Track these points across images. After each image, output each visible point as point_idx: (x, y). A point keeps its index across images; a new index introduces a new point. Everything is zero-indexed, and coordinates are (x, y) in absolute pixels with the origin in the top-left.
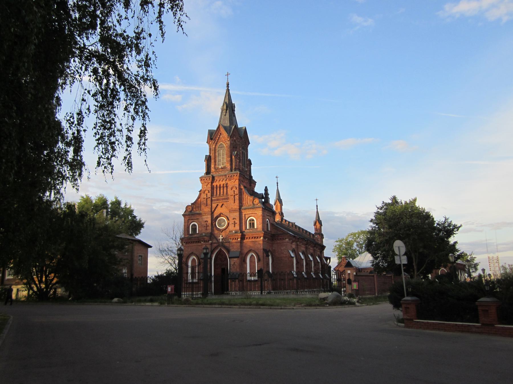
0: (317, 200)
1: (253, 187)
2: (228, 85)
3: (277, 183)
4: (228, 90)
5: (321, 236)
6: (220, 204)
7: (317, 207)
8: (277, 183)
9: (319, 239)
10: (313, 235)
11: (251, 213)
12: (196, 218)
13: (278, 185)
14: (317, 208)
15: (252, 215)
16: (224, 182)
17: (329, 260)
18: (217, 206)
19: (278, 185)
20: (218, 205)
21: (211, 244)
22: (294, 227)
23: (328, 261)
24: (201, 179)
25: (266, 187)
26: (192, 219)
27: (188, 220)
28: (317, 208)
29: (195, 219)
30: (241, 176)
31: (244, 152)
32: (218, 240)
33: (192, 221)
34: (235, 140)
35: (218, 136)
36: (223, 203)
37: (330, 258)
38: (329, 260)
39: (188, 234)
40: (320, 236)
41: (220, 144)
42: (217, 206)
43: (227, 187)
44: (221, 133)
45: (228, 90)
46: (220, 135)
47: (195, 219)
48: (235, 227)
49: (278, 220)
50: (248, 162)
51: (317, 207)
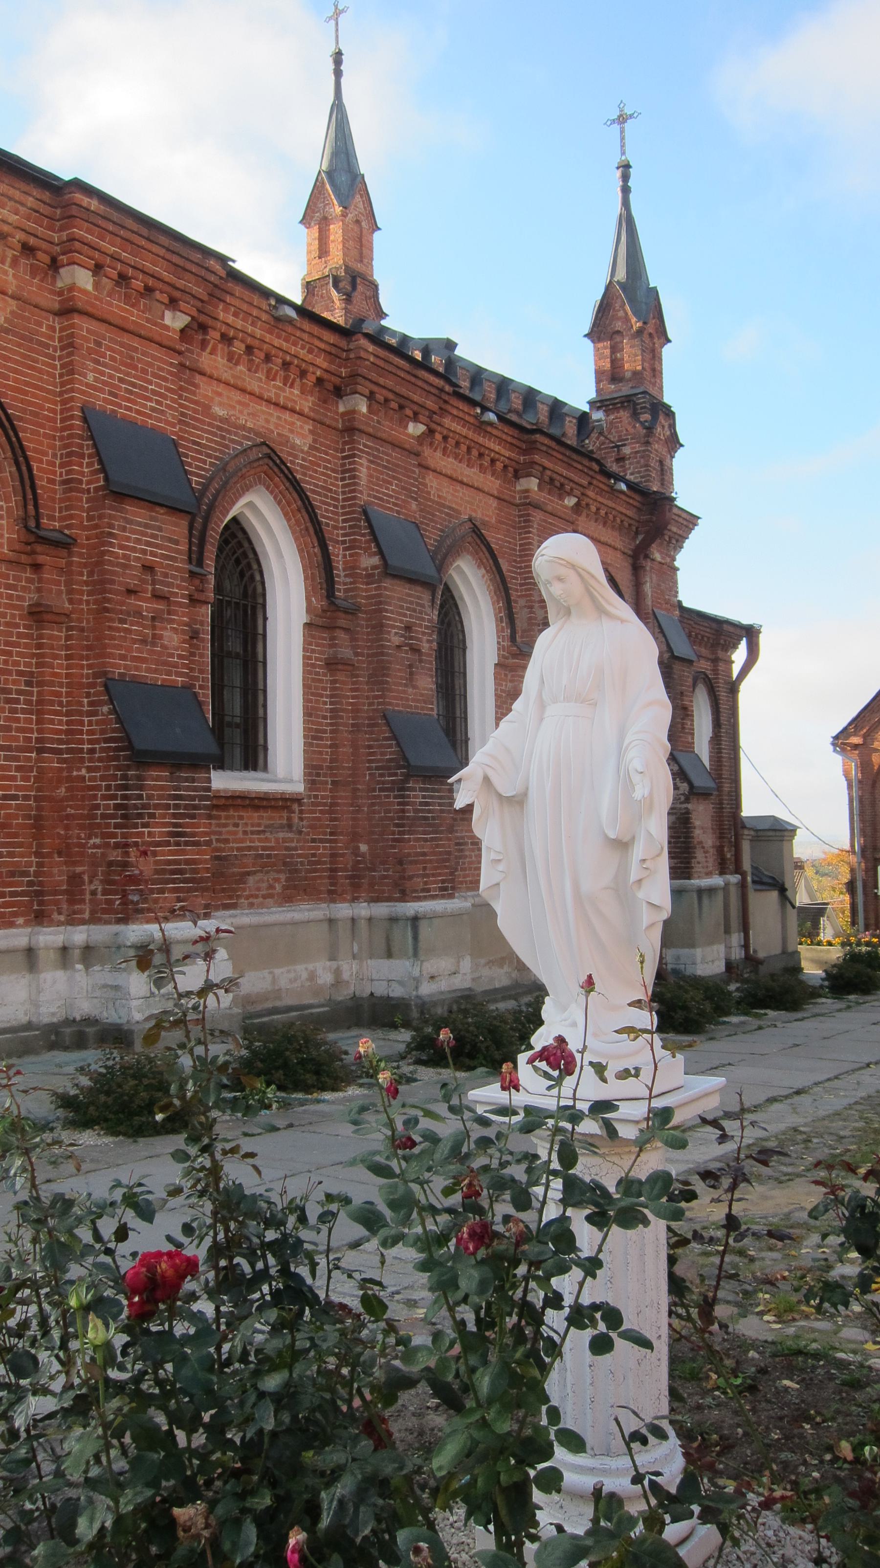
0: (622, 119)
3: (338, 58)
5: (646, 417)
7: (625, 177)
8: (338, 58)
9: (627, 450)
10: (583, 419)
13: (338, 73)
14: (626, 190)
17: (743, 645)
19: (338, 73)
23: (739, 656)
37: (751, 633)
38: (743, 645)
40: (635, 415)
51: (625, 177)
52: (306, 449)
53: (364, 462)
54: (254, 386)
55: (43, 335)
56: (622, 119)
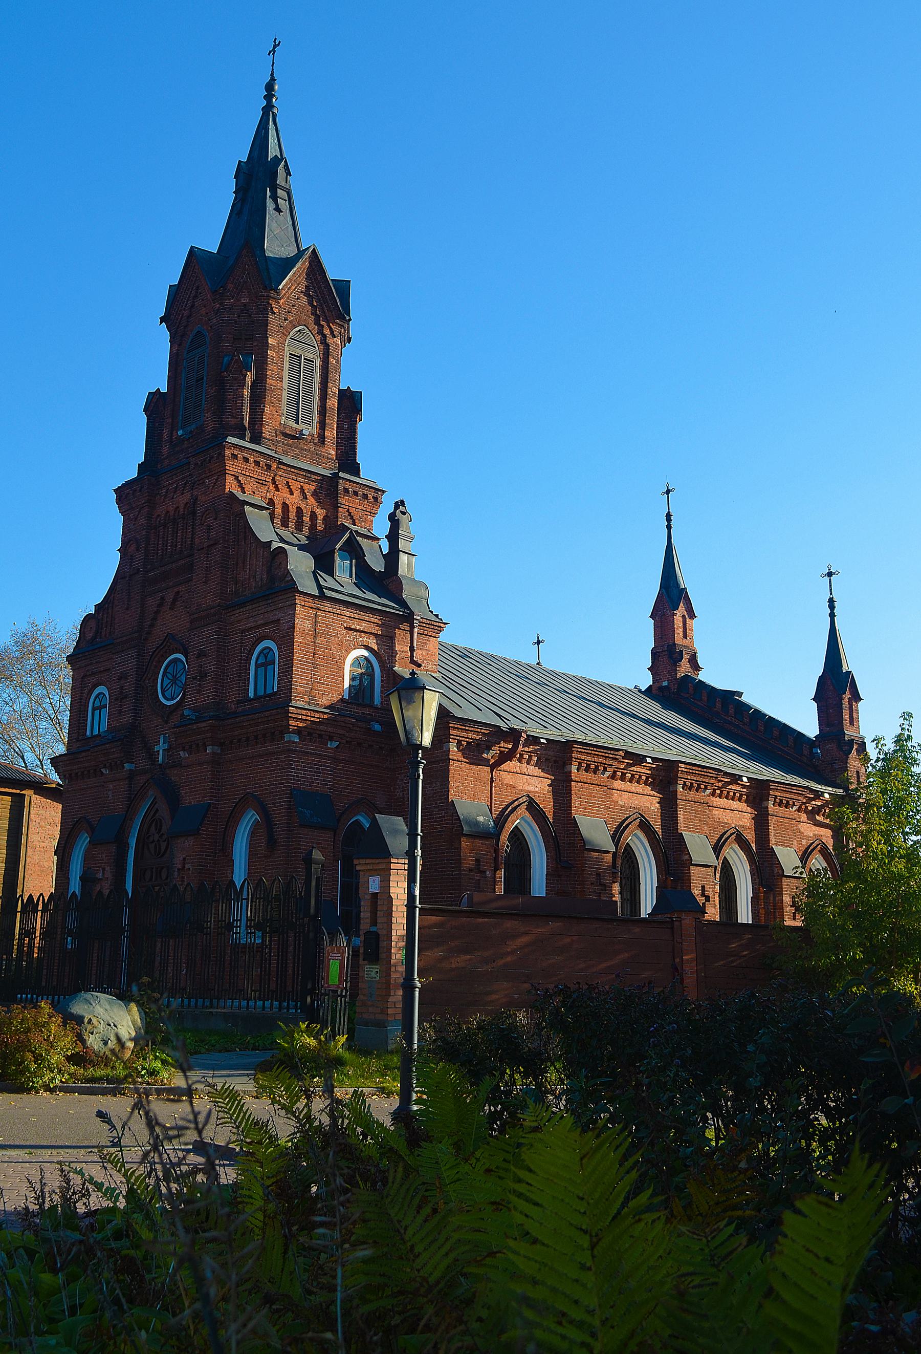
1: (356, 514)
2: (270, 87)
4: (268, 109)
6: (169, 598)
11: (259, 623)
12: (102, 669)
14: (832, 616)
15: (266, 630)
16: (187, 496)
18: (160, 605)
20: (163, 598)
21: (132, 775)
22: (732, 711)
24: (124, 494)
25: (399, 504)
26: (93, 674)
27: (82, 678)
28: (832, 616)
29: (101, 672)
30: (246, 460)
31: (310, 356)
32: (152, 756)
33: (94, 680)
34: (245, 305)
35: (189, 304)
36: (176, 590)
39: (78, 740)
41: (195, 332)
42: (160, 605)
43: (194, 513)
44: (198, 288)
45: (268, 109)
46: (196, 297)
47: (101, 672)
48: (199, 692)
49: (665, 684)
50: (333, 403)
52: (656, 810)
53: (682, 813)
54: (633, 789)
55: (561, 790)
56: (830, 574)
